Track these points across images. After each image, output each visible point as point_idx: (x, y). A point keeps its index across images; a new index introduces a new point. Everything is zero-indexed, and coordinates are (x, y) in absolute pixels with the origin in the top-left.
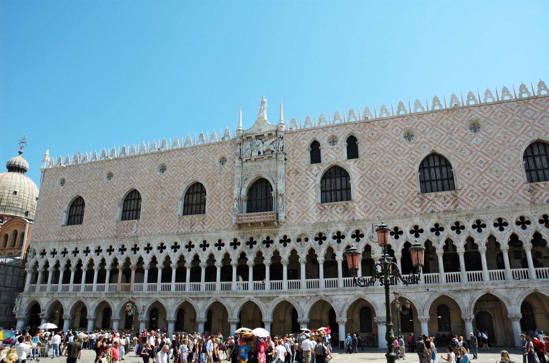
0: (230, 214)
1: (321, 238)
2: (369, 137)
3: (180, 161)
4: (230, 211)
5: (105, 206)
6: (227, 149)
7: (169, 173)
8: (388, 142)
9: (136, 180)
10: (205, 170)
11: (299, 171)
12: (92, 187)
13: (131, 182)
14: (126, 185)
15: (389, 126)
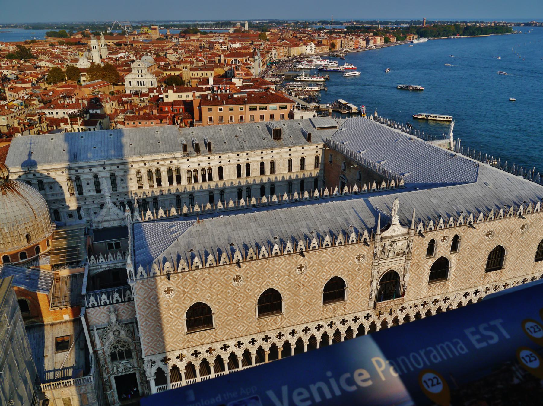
0: (366, 298)
1: (424, 304)
2: (468, 237)
3: (320, 261)
4: (366, 297)
5: (240, 308)
6: (366, 249)
7: (310, 272)
8: (478, 240)
9: (273, 281)
10: (346, 268)
11: (419, 264)
12: (218, 293)
13: (268, 284)
14: (263, 287)
15: (481, 229)
